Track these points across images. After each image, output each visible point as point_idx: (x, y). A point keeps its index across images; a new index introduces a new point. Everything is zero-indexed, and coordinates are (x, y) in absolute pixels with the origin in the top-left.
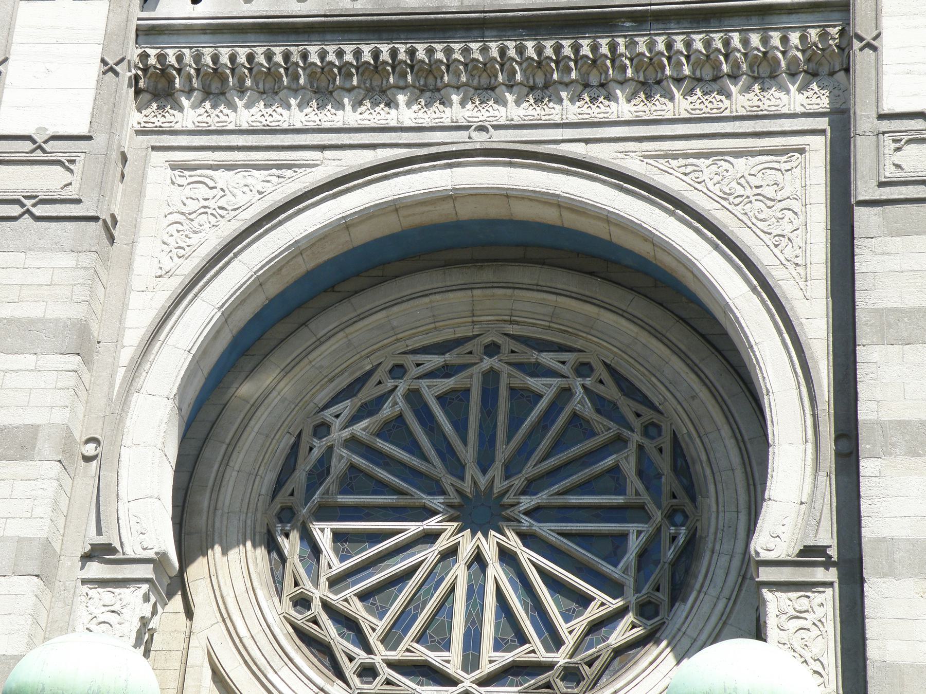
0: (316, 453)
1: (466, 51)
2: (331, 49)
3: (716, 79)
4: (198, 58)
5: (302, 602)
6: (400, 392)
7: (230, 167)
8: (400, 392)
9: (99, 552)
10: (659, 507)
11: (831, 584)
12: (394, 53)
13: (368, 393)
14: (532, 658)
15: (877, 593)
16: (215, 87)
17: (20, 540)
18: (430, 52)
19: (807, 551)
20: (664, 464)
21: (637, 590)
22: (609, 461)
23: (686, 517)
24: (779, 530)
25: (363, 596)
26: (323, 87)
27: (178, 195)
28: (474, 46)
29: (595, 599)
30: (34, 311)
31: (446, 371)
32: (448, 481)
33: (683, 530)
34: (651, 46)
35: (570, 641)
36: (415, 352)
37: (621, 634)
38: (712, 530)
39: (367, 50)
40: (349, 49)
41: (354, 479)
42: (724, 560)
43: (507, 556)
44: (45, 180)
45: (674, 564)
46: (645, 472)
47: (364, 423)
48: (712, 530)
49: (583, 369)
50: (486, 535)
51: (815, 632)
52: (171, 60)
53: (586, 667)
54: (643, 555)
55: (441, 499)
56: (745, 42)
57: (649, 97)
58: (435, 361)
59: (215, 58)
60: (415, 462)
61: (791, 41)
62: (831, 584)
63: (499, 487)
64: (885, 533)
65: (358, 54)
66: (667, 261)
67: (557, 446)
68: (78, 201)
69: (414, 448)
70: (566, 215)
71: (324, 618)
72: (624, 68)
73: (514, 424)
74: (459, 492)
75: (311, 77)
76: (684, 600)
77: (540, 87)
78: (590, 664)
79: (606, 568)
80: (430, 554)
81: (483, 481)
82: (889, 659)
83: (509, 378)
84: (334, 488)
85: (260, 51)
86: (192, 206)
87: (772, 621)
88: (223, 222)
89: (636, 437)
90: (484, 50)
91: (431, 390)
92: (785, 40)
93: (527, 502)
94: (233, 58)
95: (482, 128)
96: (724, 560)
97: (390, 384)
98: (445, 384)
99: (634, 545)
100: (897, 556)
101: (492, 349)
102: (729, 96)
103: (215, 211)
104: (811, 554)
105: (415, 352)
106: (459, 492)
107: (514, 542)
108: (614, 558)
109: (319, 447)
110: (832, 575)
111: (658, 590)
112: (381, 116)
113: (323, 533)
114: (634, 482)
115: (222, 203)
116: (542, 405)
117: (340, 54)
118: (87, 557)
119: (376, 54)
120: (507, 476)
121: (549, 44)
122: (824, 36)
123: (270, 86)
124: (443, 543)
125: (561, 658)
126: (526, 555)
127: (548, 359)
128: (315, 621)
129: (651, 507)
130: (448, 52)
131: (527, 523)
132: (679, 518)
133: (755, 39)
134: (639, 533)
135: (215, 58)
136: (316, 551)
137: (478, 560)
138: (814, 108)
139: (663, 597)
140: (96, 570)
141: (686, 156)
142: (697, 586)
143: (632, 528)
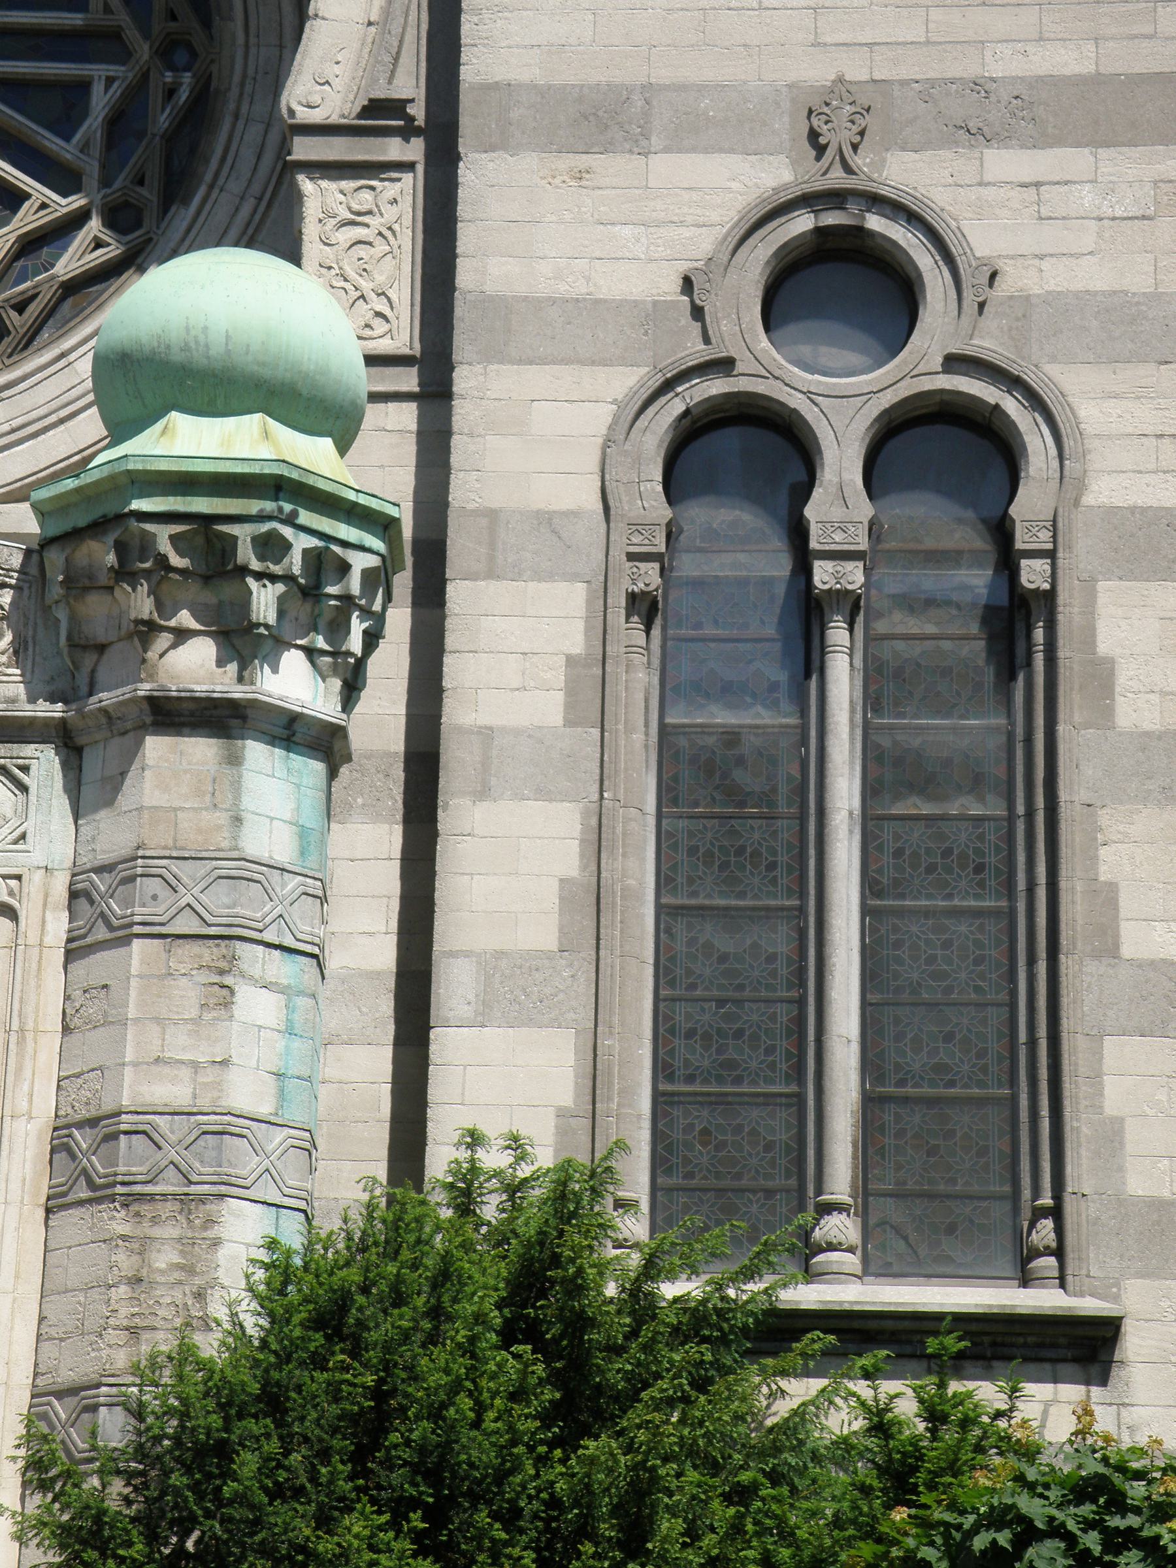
10: (146, 36)
11: (409, 166)
15: (477, 174)
19: (376, 108)
21: (105, 182)
23: (194, 54)
24: (331, 71)
29: (28, 196)
33: (187, 78)
38: (236, 78)
42: (255, 130)
45: (171, 138)
48: (236, 78)
51: (381, 247)
53: (13, 314)
54: (116, 122)
62: (409, 166)
64: (500, 74)
76: (186, 202)
78: (20, 308)
79: (51, 142)
82: (490, 288)
87: (311, 231)
96: (255, 130)
99: (100, 101)
100: (515, 114)
104: (381, 113)
108: (65, 127)
110: (415, 150)
111: (141, 183)
129: (132, 34)
132: (181, 57)
134: (110, 81)
139: (149, 194)
142: (208, 178)
143: (97, 71)
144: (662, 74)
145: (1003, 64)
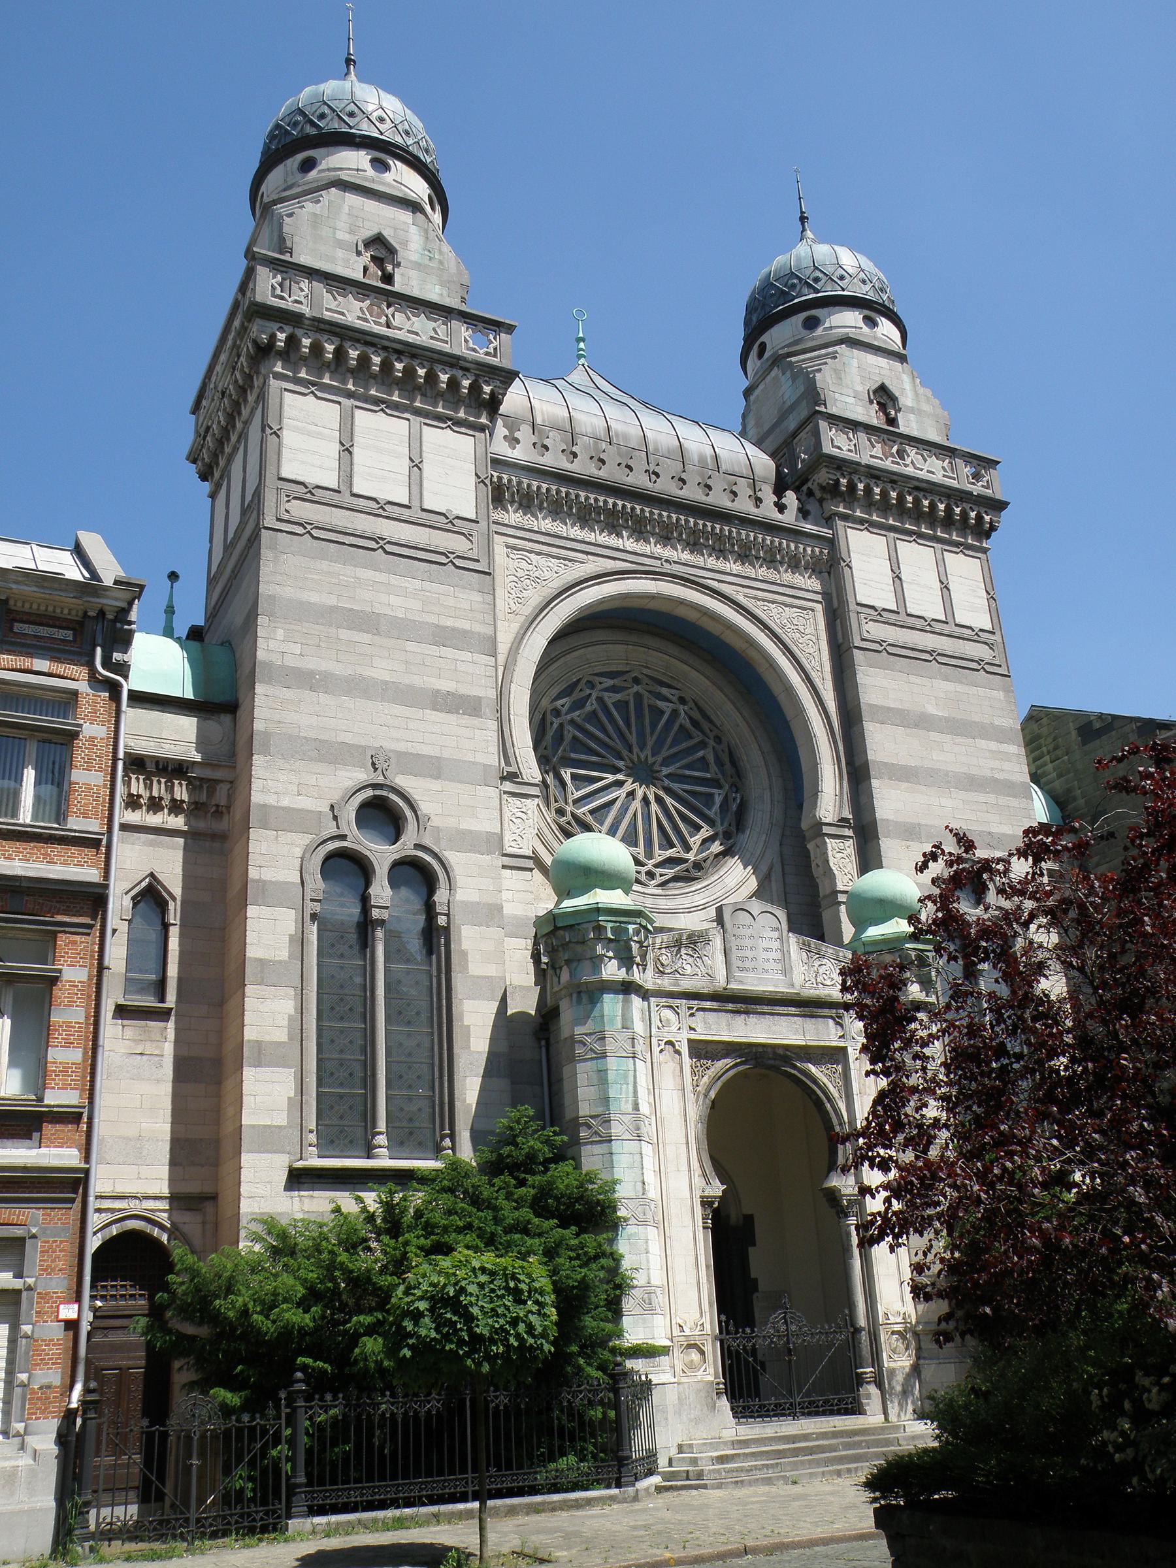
0: (555, 726)
1: (660, 515)
2: (592, 496)
3: (771, 562)
4: (519, 483)
5: (561, 812)
6: (594, 697)
7: (538, 554)
8: (594, 697)
9: (511, 777)
12: (624, 506)
13: (576, 695)
14: (678, 855)
16: (524, 502)
17: (484, 765)
18: (642, 511)
20: (726, 759)
22: (700, 754)
25: (592, 812)
26: (585, 517)
27: (513, 564)
28: (665, 514)
30: (465, 625)
31: (613, 689)
32: (625, 753)
34: (748, 536)
35: (695, 848)
36: (596, 675)
37: (716, 847)
39: (611, 501)
40: (601, 499)
41: (576, 743)
43: (659, 800)
44: (457, 544)
46: (719, 763)
47: (578, 713)
49: (682, 700)
50: (648, 787)
52: (505, 481)
55: (622, 763)
56: (788, 546)
57: (743, 564)
58: (609, 682)
59: (529, 486)
60: (607, 740)
61: (809, 550)
63: (651, 760)
65: (605, 502)
66: (752, 653)
67: (675, 742)
68: (478, 561)
69: (604, 730)
70: (704, 618)
71: (573, 823)
72: (733, 545)
73: (654, 726)
74: (631, 760)
75: (579, 510)
76: (743, 832)
77: (694, 546)
80: (622, 793)
81: (642, 756)
83: (648, 700)
84: (568, 748)
85: (554, 488)
86: (520, 573)
88: (539, 587)
89: (712, 743)
90: (669, 517)
91: (611, 699)
92: (804, 549)
93: (665, 771)
94: (539, 488)
95: (667, 561)
97: (588, 692)
98: (618, 697)
99: (718, 800)
101: (636, 681)
102: (779, 572)
103: (544, 580)
105: (596, 675)
106: (631, 760)
107: (661, 793)
109: (557, 722)
110: (849, 833)
112: (613, 541)
113: (566, 774)
114: (713, 767)
115: (537, 574)
116: (666, 717)
117: (596, 500)
118: (503, 779)
119: (615, 505)
120: (653, 755)
121: (701, 522)
122: (821, 552)
123: (557, 509)
124: (628, 787)
125: (691, 856)
126: (669, 801)
127: (665, 691)
128: (569, 823)
129: (722, 781)
130: (651, 513)
131: (666, 782)
133: (792, 546)
135: (529, 486)
136: (563, 784)
137: (645, 800)
138: (816, 589)
139: (733, 829)
140: (508, 786)
141: (764, 601)
144: (922, 822)
145: (995, 829)
